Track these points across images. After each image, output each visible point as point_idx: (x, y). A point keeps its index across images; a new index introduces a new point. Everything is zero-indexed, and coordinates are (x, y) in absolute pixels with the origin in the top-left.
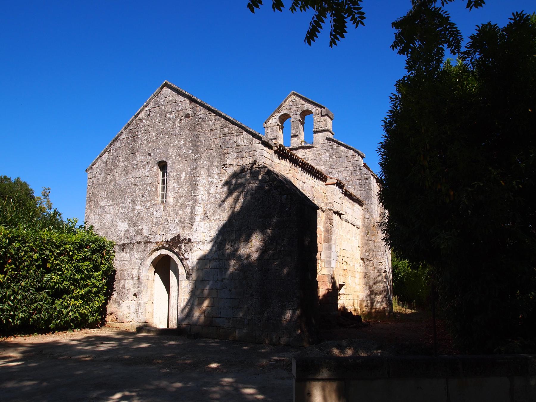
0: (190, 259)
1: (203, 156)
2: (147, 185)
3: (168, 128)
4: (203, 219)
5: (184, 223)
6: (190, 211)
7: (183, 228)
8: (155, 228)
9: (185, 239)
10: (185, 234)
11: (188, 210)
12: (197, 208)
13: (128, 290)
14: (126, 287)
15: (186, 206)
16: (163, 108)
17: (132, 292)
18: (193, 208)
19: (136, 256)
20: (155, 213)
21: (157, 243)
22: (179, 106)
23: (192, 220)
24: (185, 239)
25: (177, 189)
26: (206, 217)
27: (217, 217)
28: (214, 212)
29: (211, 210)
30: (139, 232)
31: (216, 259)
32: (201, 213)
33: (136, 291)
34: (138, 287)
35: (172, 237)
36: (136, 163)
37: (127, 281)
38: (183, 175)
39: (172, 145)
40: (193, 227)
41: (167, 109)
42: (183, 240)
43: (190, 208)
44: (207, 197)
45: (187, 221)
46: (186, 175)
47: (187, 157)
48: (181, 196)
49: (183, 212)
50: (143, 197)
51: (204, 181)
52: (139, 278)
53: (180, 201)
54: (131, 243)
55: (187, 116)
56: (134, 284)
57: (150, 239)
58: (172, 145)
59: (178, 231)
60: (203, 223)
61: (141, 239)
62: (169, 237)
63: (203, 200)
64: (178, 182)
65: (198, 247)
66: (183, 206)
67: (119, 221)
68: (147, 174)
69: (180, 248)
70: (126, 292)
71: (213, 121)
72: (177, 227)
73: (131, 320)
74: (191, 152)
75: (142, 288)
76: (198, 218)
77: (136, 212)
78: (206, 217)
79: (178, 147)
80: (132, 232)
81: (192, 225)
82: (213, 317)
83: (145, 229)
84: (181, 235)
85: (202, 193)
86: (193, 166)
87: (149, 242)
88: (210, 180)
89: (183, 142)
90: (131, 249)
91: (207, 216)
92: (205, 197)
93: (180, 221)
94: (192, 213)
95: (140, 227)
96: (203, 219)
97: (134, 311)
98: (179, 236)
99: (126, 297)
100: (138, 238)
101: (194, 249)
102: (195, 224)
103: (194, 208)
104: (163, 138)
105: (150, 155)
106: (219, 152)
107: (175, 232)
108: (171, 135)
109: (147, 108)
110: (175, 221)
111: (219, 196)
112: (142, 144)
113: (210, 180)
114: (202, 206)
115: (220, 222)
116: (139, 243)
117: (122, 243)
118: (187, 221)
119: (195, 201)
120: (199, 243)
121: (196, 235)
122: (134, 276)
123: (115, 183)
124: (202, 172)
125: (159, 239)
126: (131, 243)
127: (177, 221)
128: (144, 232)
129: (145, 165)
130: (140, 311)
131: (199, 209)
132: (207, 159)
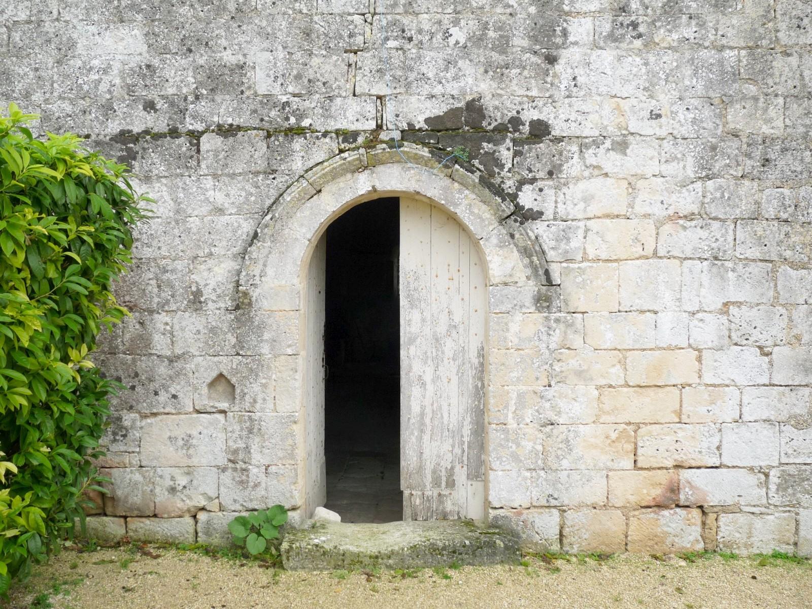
0: (549, 214)
4: (612, 37)
5: (503, 46)
7: (497, 71)
8: (327, 66)
9: (516, 122)
10: (504, 98)
13: (172, 360)
17: (204, 368)
19: (219, 198)
21: (349, 136)
24: (516, 122)
27: (689, 31)
30: (222, 80)
31: (689, 217)
33: (226, 364)
34: (240, 343)
35: (437, 109)
37: (161, 319)
40: (559, 67)
42: (501, 130)
45: (520, 41)
54: (174, 133)
56: (213, 330)
57: (301, 117)
59: (472, 82)
60: (607, 56)
61: (238, 111)
62: (420, 110)
67: (87, 20)
70: (163, 370)
73: (203, 503)
75: (265, 349)
80: (178, 76)
81: (551, 60)
82: (677, 467)
83: (266, 71)
84: (489, 103)
87: (300, 131)
91: (634, 25)
93: (478, 40)
95: (229, 58)
96: (612, 37)
97: (222, 461)
98: (474, 109)
99: (163, 397)
100: (224, 111)
101: (573, 167)
107: (453, 88)
110: (447, 35)
115: (704, 53)
116: (227, 131)
117: (114, 127)
118: (520, 41)
120: (596, 144)
121: (578, 104)
122: (207, 293)
125: (354, 116)
126: (174, 133)
127: (459, 35)
128: (261, 81)
130: (257, 457)
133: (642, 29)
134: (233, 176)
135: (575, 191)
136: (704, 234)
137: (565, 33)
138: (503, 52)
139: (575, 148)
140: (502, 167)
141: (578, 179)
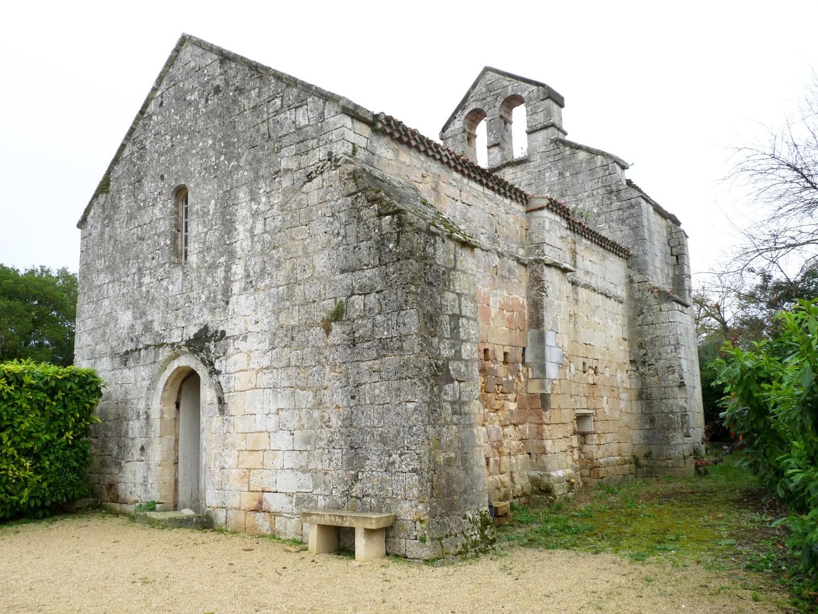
0: (223, 372)
1: (242, 162)
2: (159, 236)
3: (187, 122)
4: (245, 289)
5: (214, 301)
6: (223, 275)
7: (212, 311)
8: (170, 317)
9: (216, 332)
10: (216, 323)
11: (220, 273)
12: (234, 267)
14: (130, 435)
15: (217, 267)
16: (181, 86)
18: (228, 270)
19: (143, 373)
20: (171, 287)
22: (205, 75)
23: (227, 292)
24: (216, 332)
25: (203, 235)
26: (250, 284)
27: (267, 282)
28: (263, 271)
29: (258, 269)
31: (267, 368)
32: (240, 277)
36: (143, 198)
38: (212, 207)
39: (194, 151)
40: (229, 306)
41: (186, 86)
43: (223, 268)
44: (250, 244)
45: (219, 297)
46: (216, 205)
47: (217, 170)
48: (209, 249)
49: (213, 278)
50: (153, 259)
51: (245, 212)
52: (148, 417)
53: (208, 259)
55: (217, 90)
56: (141, 427)
58: (194, 151)
59: (207, 318)
60: (243, 297)
62: (192, 331)
63: (243, 250)
64: (204, 222)
65: (236, 346)
66: (213, 267)
68: (159, 216)
69: (209, 350)
71: (257, 90)
72: (204, 309)
74: (223, 158)
76: (236, 287)
77: (144, 289)
78: (250, 284)
79: (203, 154)
80: (139, 328)
81: (227, 303)
84: (210, 325)
85: (242, 236)
86: (227, 185)
88: (255, 207)
89: (210, 142)
90: (137, 360)
91: (251, 282)
92: (247, 244)
93: (208, 298)
94: (226, 279)
95: (150, 318)
96: (245, 289)
97: (142, 482)
98: (206, 328)
99: (130, 455)
100: (147, 340)
101: (231, 350)
102: (233, 300)
103: (230, 269)
104: (181, 142)
105: (162, 177)
106: (268, 149)
107: (201, 320)
108: (192, 134)
109: (159, 93)
110: (200, 298)
111: (269, 238)
112: (151, 160)
113: (255, 207)
114: (242, 262)
116: (147, 347)
117: (124, 350)
118: (219, 297)
119: (231, 254)
122: (141, 413)
123: (116, 240)
124: (241, 195)
126: (136, 350)
127: (203, 298)
128: (157, 327)
129: (156, 199)
130: (150, 481)
131: (238, 270)
132: (248, 167)
133: (254, 283)
134: (146, 365)
135: (231, 360)
136: (271, 376)
137: (231, 290)
138: (215, 302)
139: (232, 341)
140: (210, 352)
141: (232, 355)
